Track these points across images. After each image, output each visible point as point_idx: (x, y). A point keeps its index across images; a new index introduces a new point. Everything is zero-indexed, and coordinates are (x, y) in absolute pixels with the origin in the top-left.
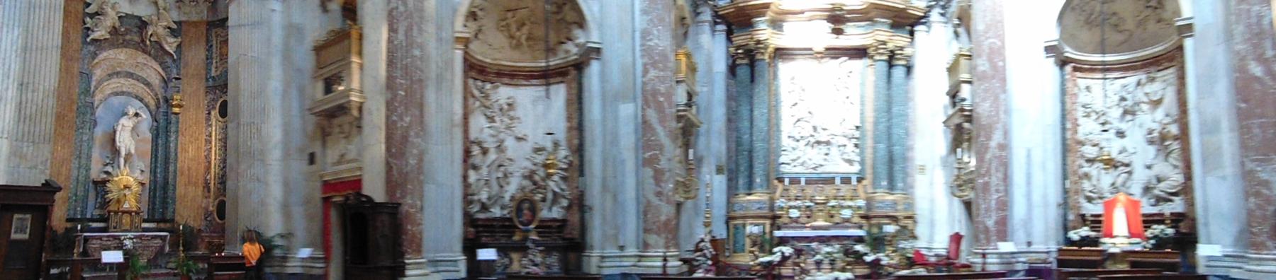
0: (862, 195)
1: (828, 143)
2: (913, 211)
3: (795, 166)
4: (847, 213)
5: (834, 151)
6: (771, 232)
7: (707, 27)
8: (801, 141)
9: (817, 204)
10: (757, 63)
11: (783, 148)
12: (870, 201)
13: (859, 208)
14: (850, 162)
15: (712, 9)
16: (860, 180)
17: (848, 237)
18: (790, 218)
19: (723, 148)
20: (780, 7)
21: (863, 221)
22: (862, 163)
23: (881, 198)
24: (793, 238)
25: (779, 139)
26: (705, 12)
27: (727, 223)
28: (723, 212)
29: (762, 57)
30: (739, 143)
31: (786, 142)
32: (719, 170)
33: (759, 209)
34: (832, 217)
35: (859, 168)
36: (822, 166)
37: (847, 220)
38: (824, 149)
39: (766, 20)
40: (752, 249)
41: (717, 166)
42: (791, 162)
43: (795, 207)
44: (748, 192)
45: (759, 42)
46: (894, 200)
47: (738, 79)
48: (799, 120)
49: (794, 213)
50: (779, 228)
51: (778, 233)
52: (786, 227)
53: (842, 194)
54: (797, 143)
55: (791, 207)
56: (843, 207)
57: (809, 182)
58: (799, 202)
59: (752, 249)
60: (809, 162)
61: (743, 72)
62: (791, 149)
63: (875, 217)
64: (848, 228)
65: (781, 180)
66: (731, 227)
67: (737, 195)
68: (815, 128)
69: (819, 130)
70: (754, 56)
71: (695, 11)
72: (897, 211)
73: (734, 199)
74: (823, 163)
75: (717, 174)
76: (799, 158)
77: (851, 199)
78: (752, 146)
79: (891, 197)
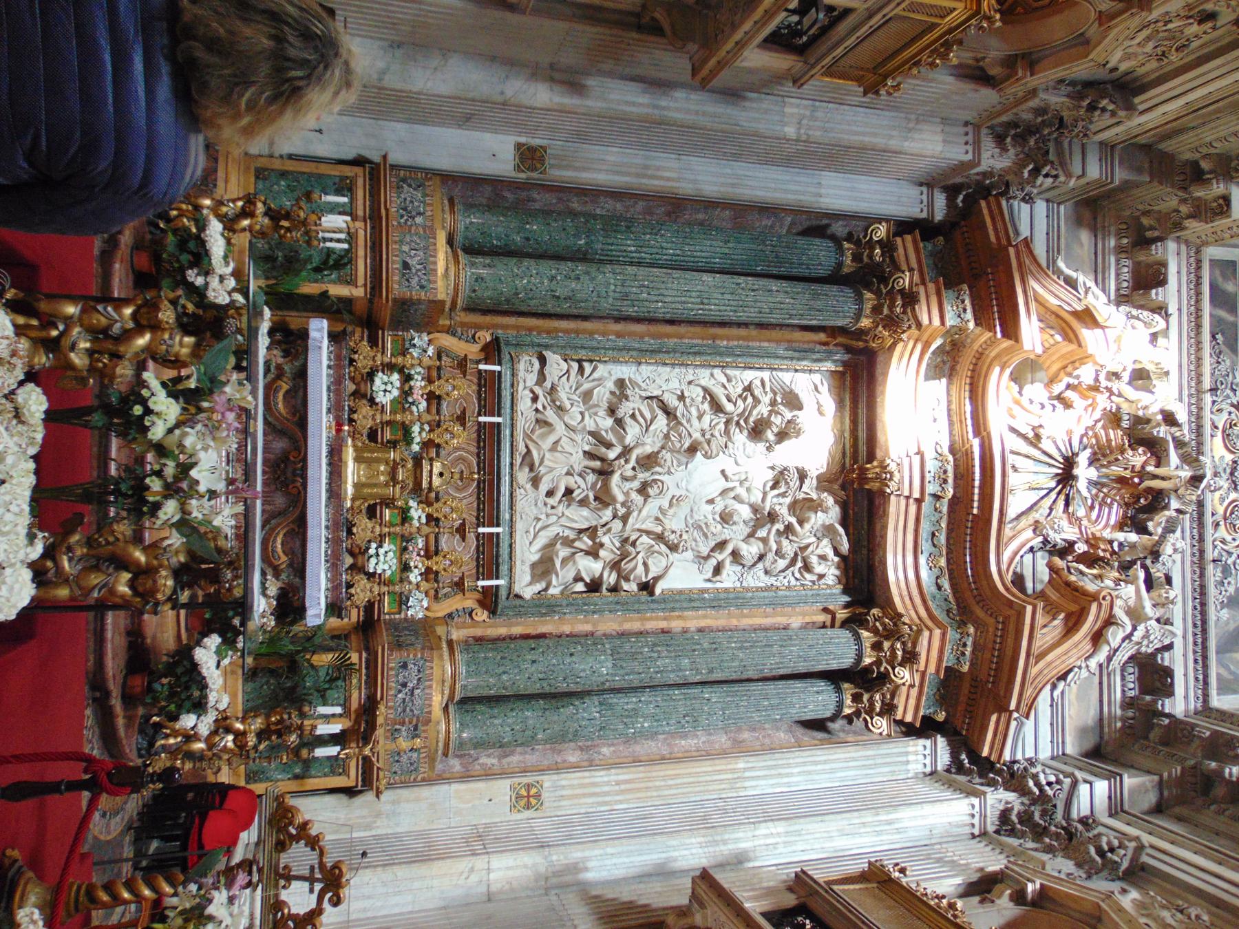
0: (442, 609)
1: (603, 499)
2: (390, 786)
3: (535, 399)
4: (384, 561)
5: (581, 517)
6: (321, 305)
7: (958, 153)
8: (609, 422)
9: (418, 461)
10: (849, 292)
11: (588, 368)
12: (424, 630)
13: (402, 601)
14: (543, 568)
15: (1006, 171)
16: (489, 600)
17: (299, 569)
18: (371, 376)
19: (600, 177)
20: (997, 370)
21: (355, 616)
22: (544, 606)
23: (436, 672)
24: (301, 375)
25: (619, 353)
26: (1004, 149)
27: (359, 162)
28: (396, 157)
29: (868, 306)
30: (612, 224)
31: (609, 373)
32: (529, 156)
33: (406, 266)
34: (371, 512)
35: (528, 593)
36: (535, 482)
37: (359, 553)
38: (584, 486)
39: (961, 330)
40: (260, 208)
41: (544, 148)
42: (548, 384)
43: (406, 393)
44: (459, 239)
45: (910, 299)
46: (428, 722)
47: (802, 241)
48: (669, 412)
49: (386, 388)
50: (334, 337)
51: (319, 329)
52: (338, 358)
53: (444, 545)
54: (605, 405)
55: (407, 378)
56: (404, 541)
57: (488, 439)
58: (423, 405)
59: (260, 208)
60: (547, 444)
61: (820, 255)
62: (586, 386)
63: (372, 665)
64: (333, 562)
65: (492, 351)
66: (348, 171)
67: (451, 202)
68: (649, 461)
69: (643, 476)
70: (868, 286)
71: (1014, 124)
72: (393, 734)
73: (438, 195)
74: (544, 487)
75: (519, 146)
76: (560, 409)
77: (428, 574)
78: (601, 261)
79: (437, 712)
